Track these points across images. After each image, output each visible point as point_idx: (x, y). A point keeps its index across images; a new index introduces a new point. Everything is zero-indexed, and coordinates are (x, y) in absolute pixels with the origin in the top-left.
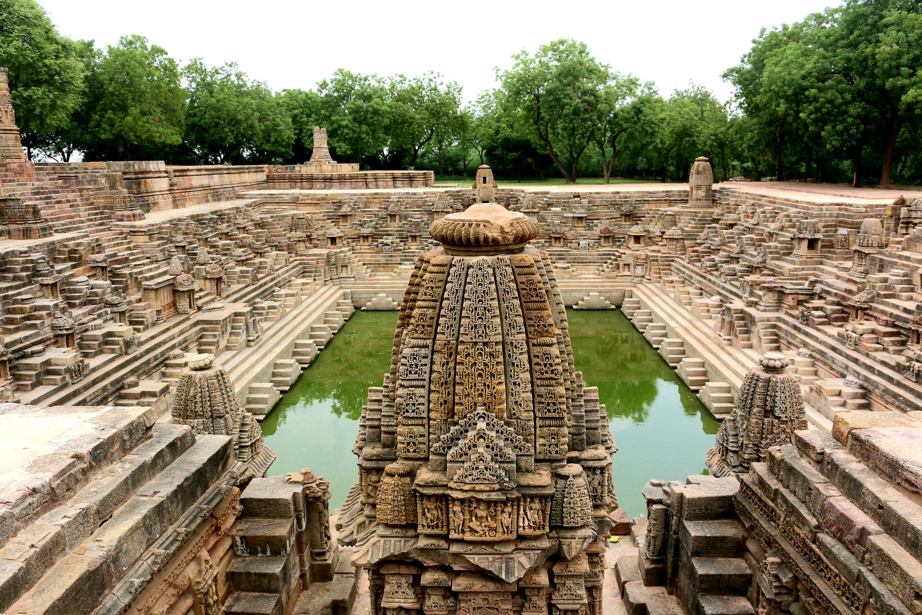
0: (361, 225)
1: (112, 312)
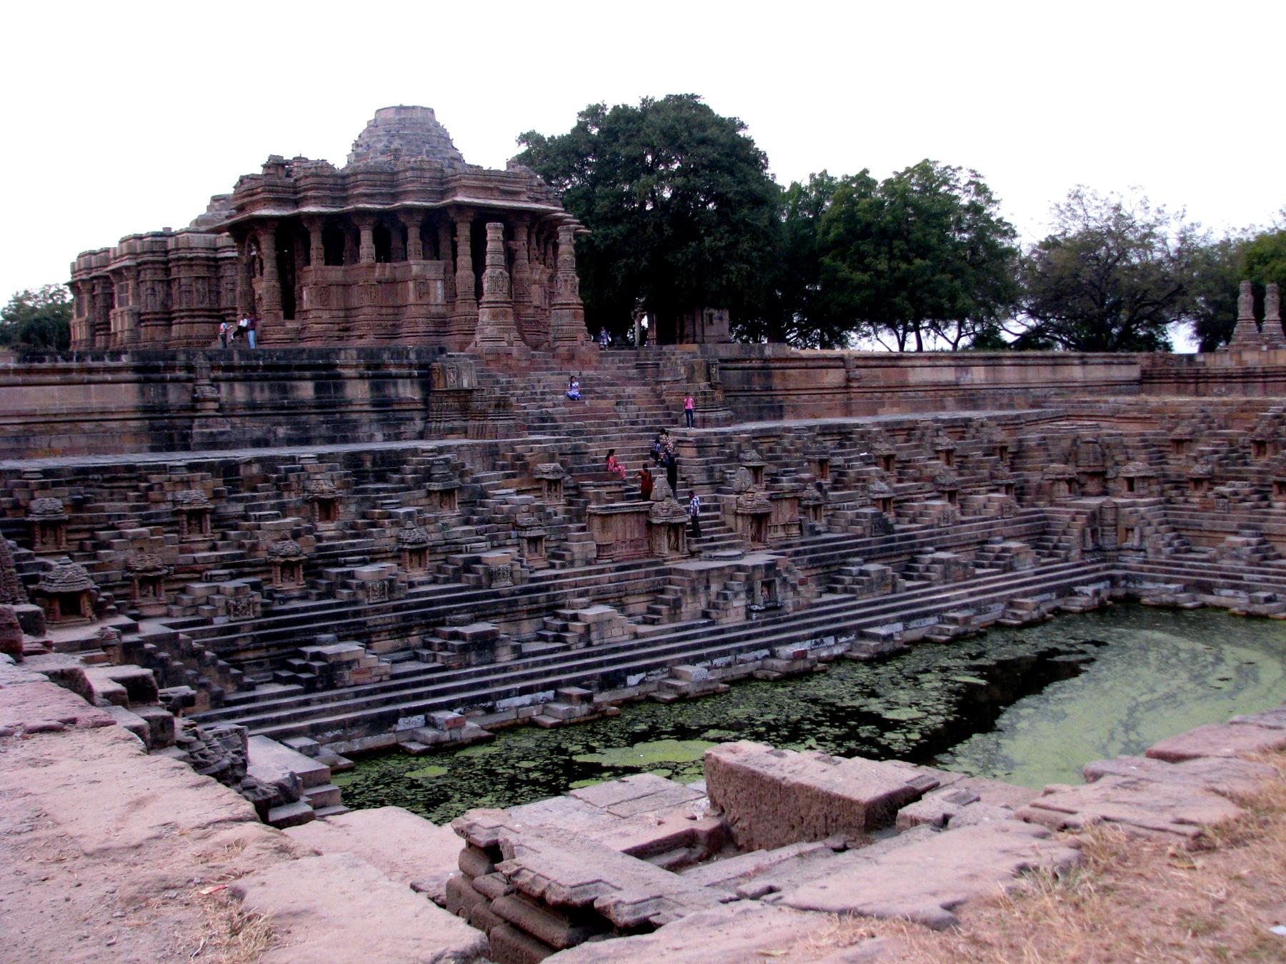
0: (1195, 459)
1: (518, 537)
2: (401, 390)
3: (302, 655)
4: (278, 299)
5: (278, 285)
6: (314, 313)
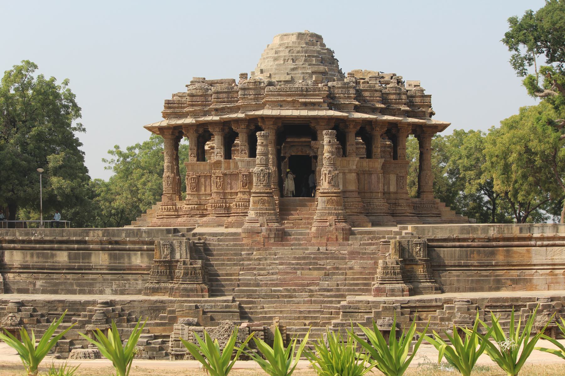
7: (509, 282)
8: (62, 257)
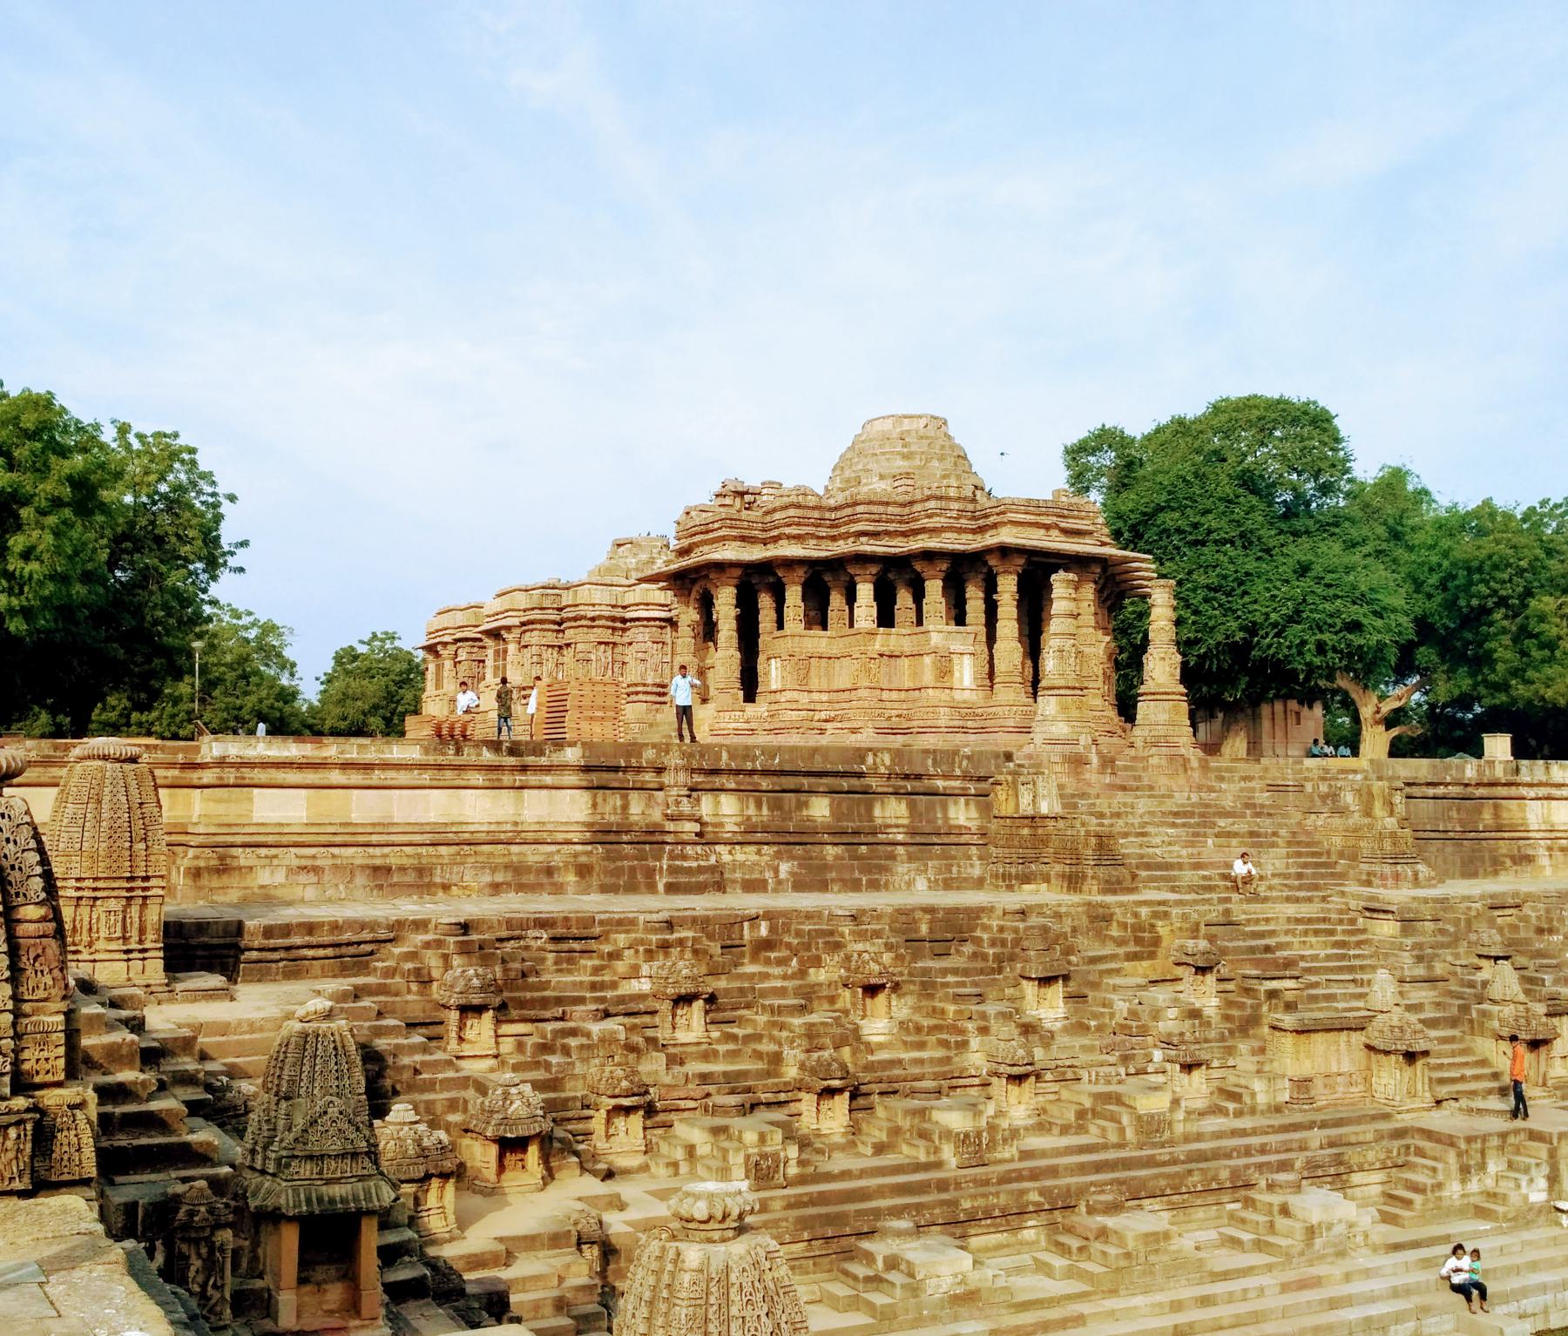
2: (952, 813)
3: (869, 1258)
4: (737, 674)
5: (738, 655)
6: (789, 695)
7: (1508, 862)
8: (820, 809)
